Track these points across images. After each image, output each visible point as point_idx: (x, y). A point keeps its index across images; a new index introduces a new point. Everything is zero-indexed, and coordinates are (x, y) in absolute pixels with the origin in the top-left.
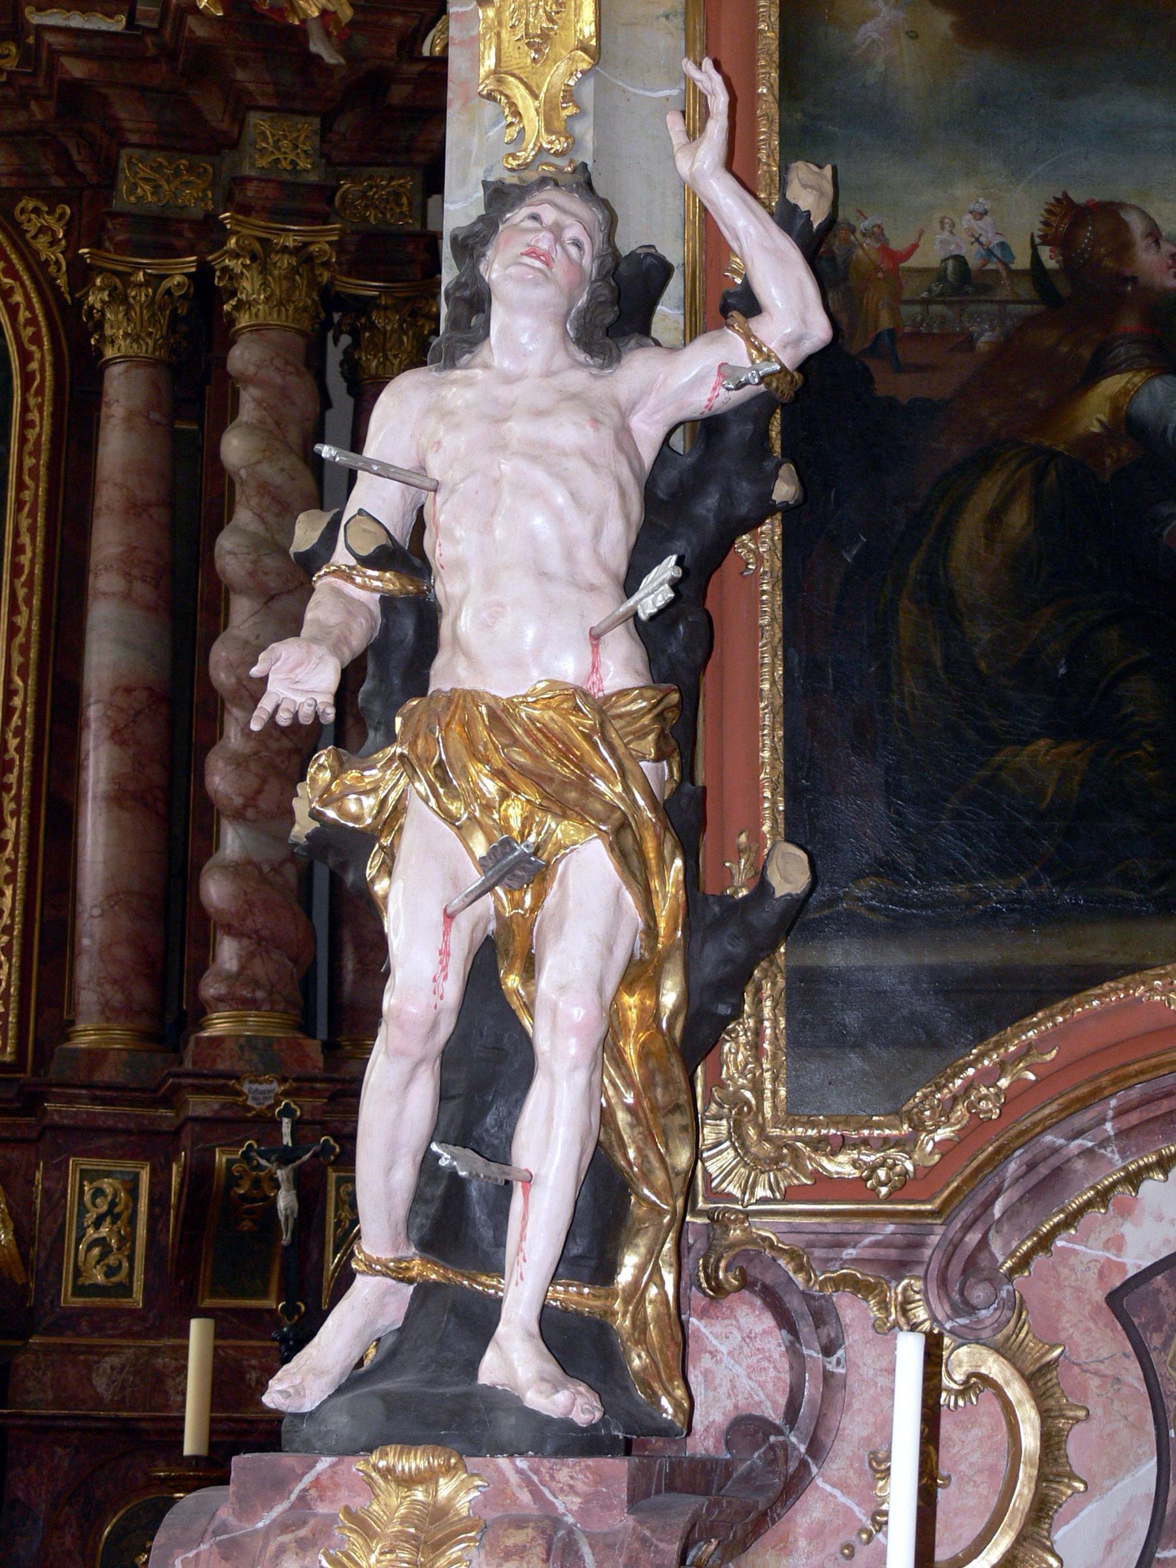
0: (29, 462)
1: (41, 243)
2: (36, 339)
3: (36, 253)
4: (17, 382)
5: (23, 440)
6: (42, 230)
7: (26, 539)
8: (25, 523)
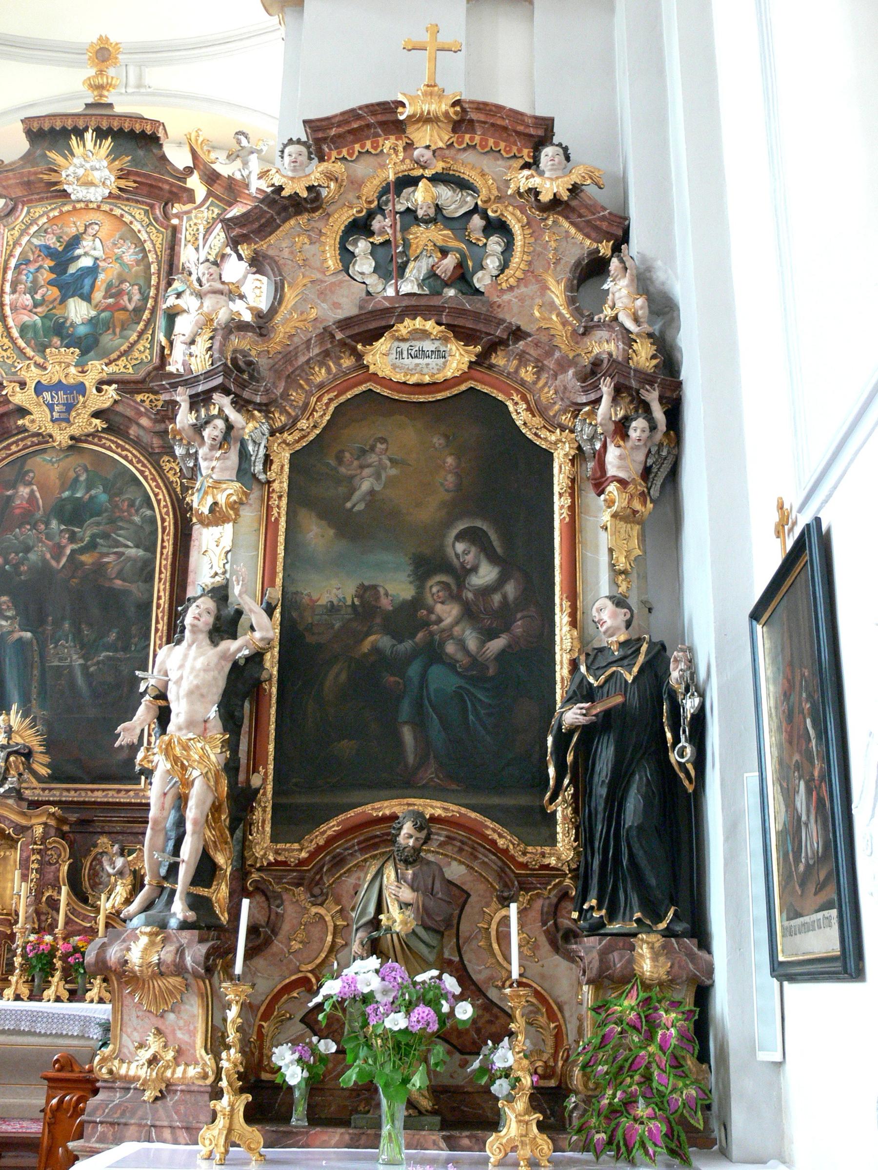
0: (164, 562)
1: (170, 475)
2: (167, 513)
3: (168, 479)
4: (160, 530)
5: (162, 554)
6: (171, 469)
7: (162, 594)
8: (162, 587)
